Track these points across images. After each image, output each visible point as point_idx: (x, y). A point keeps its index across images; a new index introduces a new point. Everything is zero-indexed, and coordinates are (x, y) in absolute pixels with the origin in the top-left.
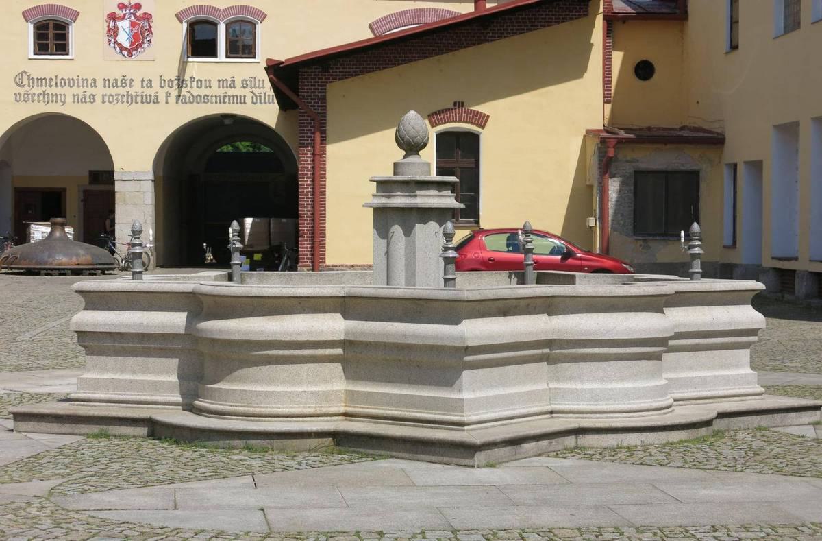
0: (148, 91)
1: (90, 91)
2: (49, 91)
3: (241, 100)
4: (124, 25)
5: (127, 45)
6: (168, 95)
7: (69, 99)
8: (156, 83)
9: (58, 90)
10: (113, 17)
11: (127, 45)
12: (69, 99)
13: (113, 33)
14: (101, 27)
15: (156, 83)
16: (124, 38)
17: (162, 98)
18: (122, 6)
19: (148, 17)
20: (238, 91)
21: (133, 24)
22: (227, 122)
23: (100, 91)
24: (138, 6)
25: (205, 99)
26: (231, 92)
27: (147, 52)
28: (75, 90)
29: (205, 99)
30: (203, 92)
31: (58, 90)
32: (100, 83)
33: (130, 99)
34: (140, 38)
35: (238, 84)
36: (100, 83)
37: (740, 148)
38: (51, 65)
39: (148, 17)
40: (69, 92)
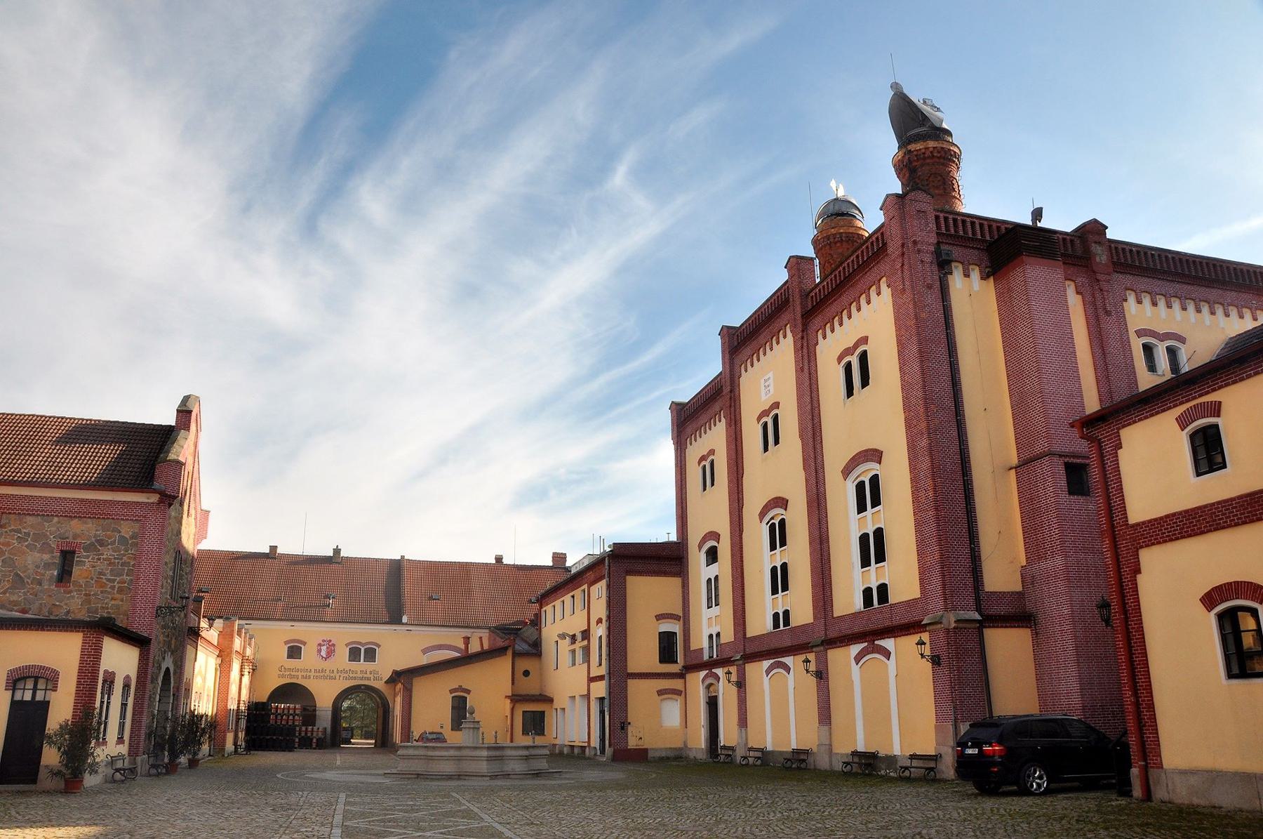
0: (332, 675)
1: (308, 674)
2: (293, 674)
3: (369, 679)
4: (324, 648)
5: (325, 656)
6: (340, 676)
7: (300, 677)
8: (335, 671)
9: (296, 674)
10: (320, 645)
11: (325, 656)
12: (300, 677)
13: (319, 651)
14: (315, 648)
15: (335, 671)
16: (324, 653)
17: (337, 677)
18: (324, 641)
19: (334, 645)
20: (368, 675)
21: (327, 648)
22: (362, 687)
23: (312, 674)
24: (330, 641)
25: (355, 678)
26: (365, 676)
27: (332, 659)
28: (303, 674)
29: (355, 678)
30: (354, 675)
31: (296, 674)
32: (313, 670)
33: (325, 678)
34: (330, 653)
35: (368, 673)
36: (313, 670)
37: (556, 704)
38: (293, 663)
39: (334, 645)
40: (300, 674)
